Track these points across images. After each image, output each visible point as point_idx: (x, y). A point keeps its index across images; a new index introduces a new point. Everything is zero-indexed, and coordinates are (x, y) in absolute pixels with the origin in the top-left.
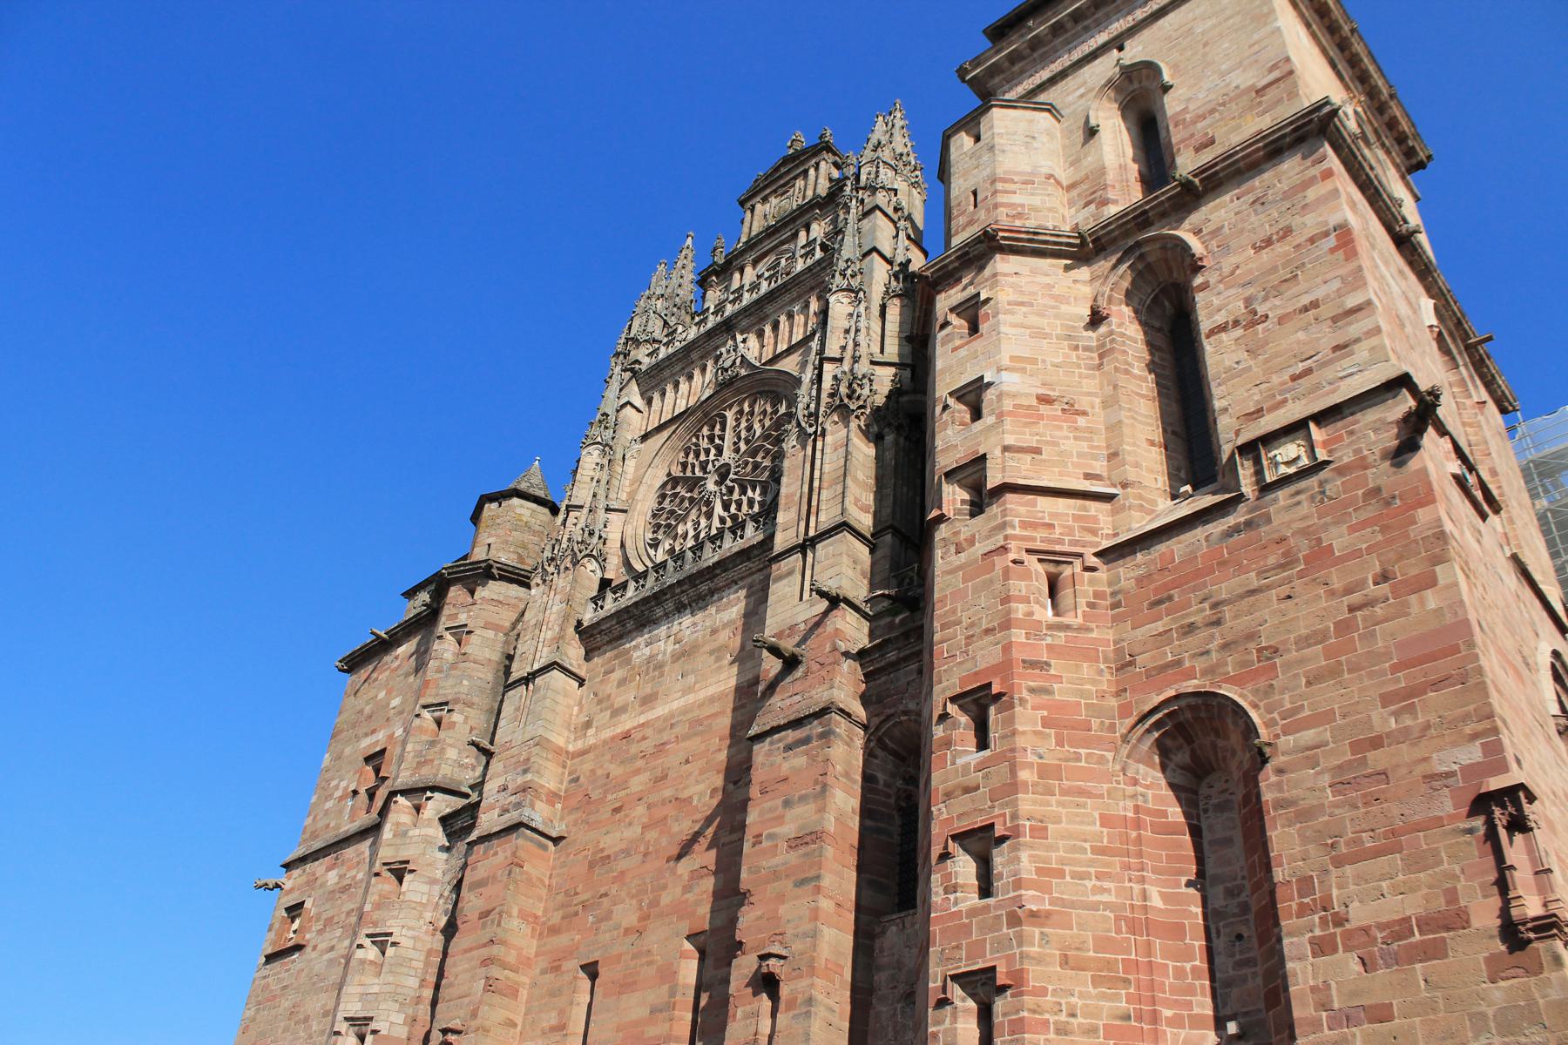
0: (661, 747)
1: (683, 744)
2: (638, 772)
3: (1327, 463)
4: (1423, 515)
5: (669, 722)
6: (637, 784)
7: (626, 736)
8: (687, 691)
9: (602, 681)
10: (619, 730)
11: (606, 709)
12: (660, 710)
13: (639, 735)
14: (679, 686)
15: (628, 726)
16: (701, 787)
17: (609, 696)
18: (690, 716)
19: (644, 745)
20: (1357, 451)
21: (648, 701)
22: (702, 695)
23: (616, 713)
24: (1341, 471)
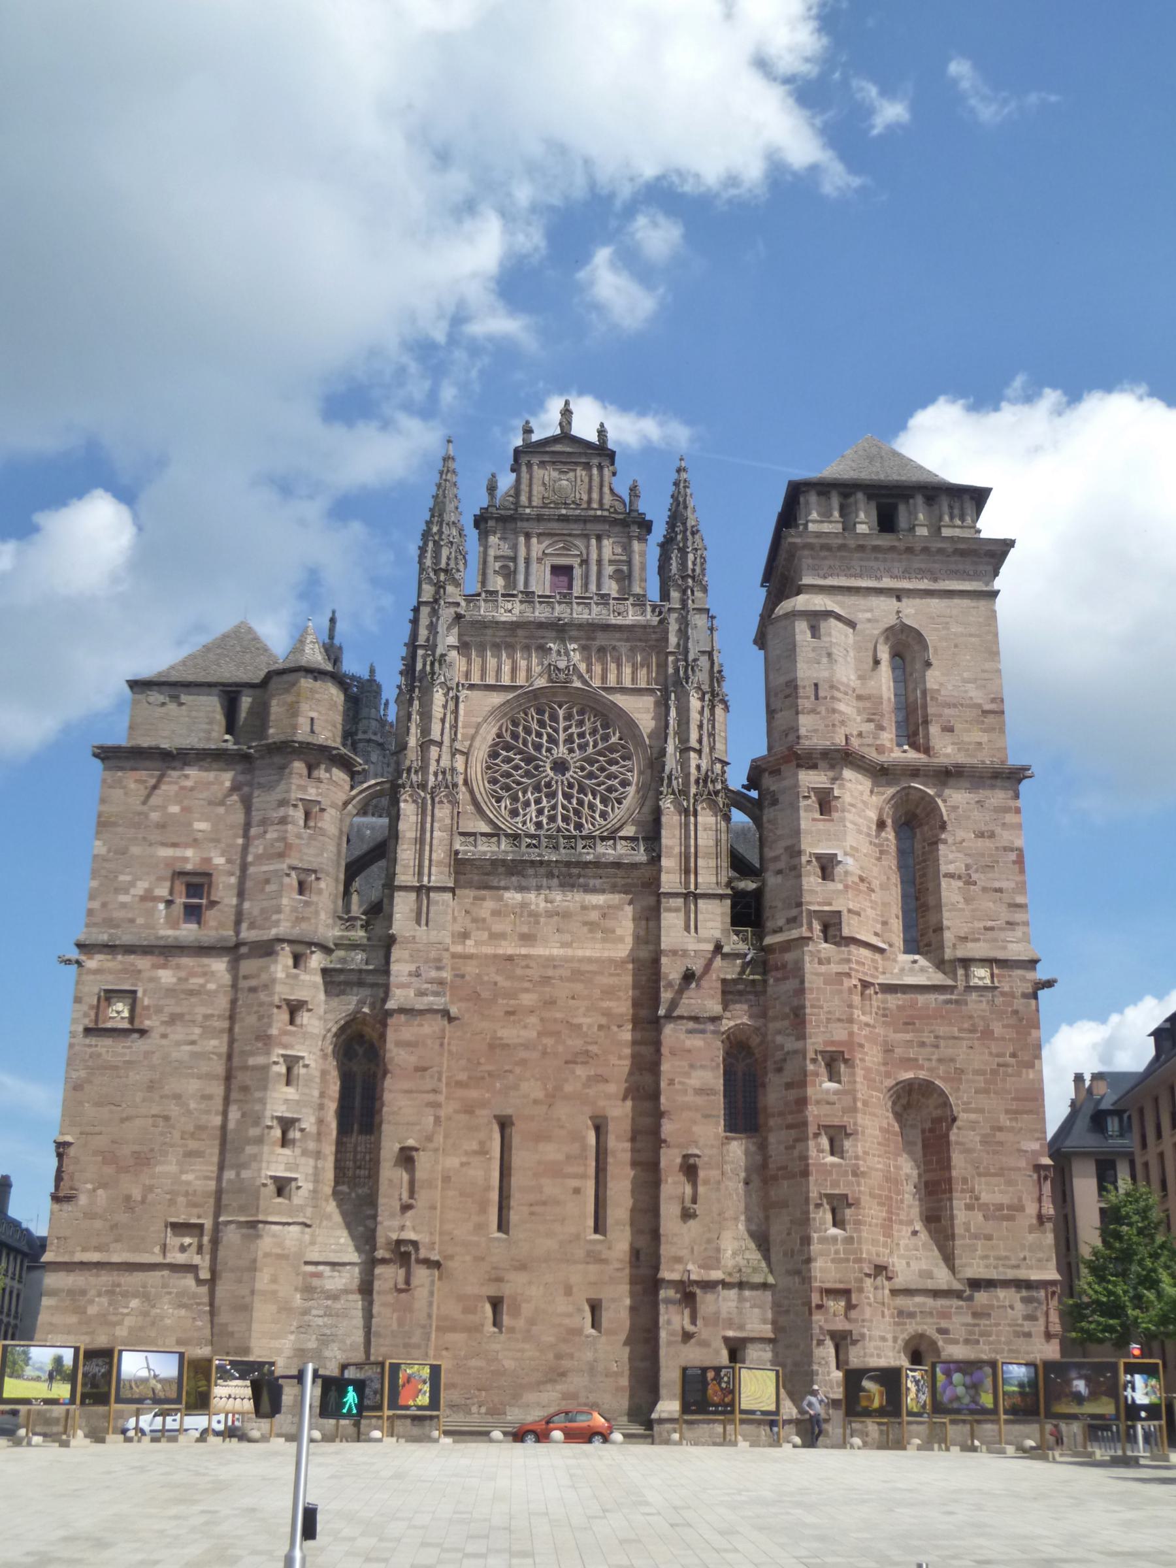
0: (546, 980)
1: (567, 984)
2: (527, 990)
3: (997, 988)
4: (1033, 1032)
5: (550, 962)
6: (528, 999)
7: (510, 958)
8: (564, 945)
9: (473, 904)
10: (500, 951)
11: (483, 929)
12: (539, 951)
13: (524, 963)
14: (557, 936)
15: (510, 951)
16: (588, 1020)
17: (484, 920)
18: (571, 965)
19: (529, 972)
20: (1011, 987)
21: (527, 938)
22: (580, 953)
23: (495, 937)
24: (1003, 994)
